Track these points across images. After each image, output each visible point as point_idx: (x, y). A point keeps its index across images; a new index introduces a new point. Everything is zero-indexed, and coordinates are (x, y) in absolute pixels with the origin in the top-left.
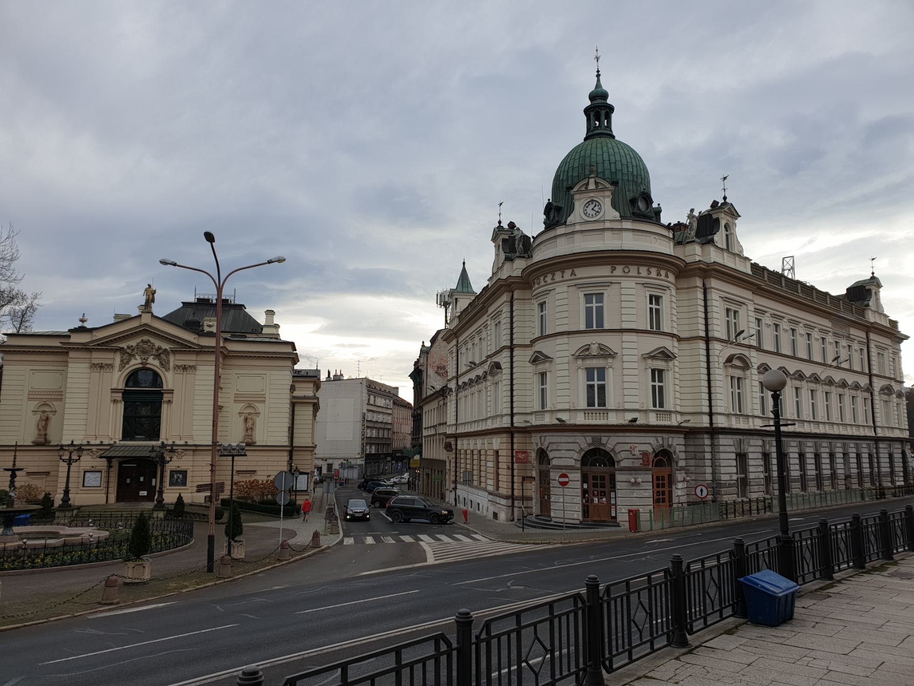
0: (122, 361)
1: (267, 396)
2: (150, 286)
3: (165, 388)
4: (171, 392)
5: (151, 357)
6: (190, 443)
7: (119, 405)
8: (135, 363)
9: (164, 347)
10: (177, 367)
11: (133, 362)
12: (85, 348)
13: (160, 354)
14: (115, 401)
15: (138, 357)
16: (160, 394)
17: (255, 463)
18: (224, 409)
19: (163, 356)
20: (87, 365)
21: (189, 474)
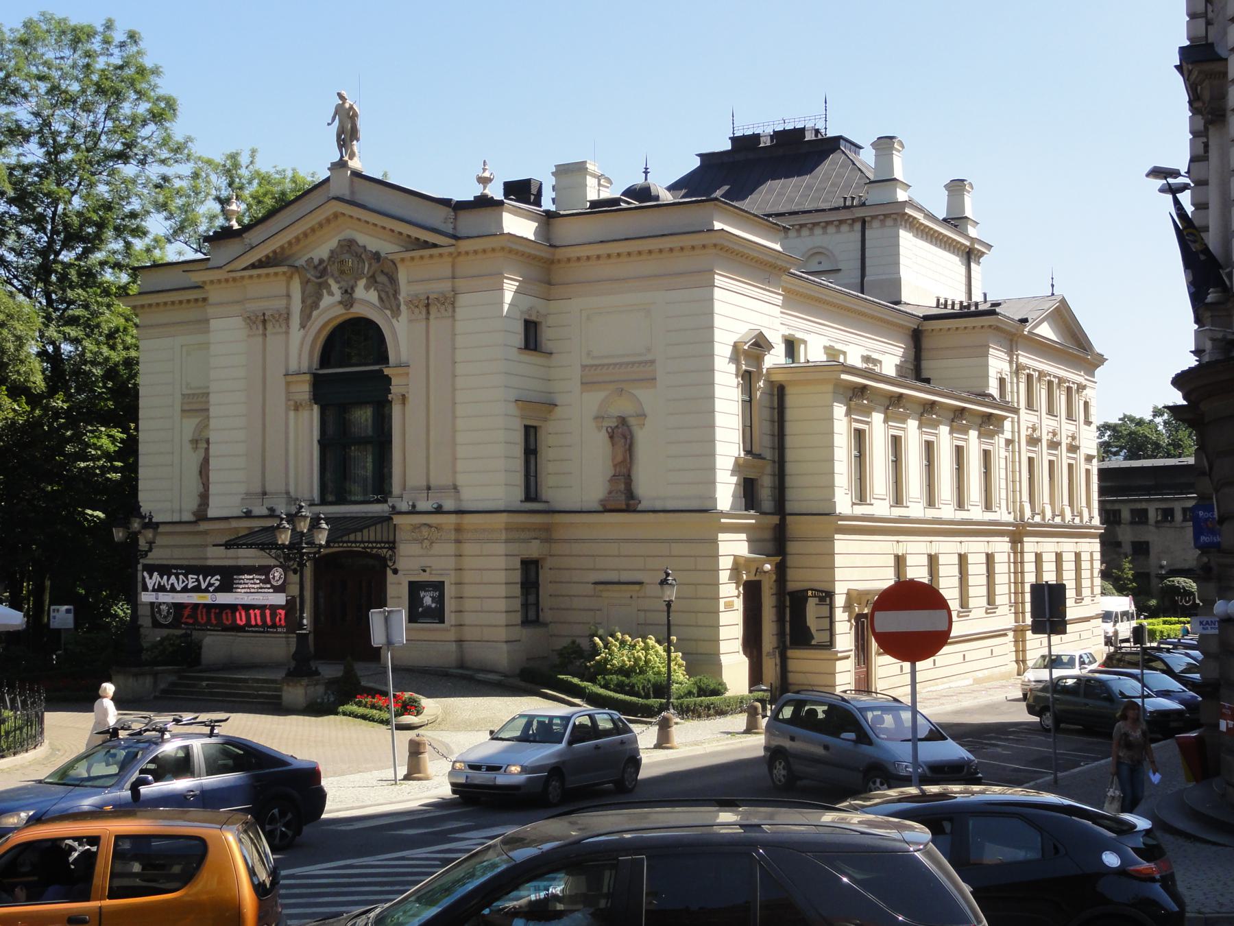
5: (362, 283)
11: (326, 301)
15: (335, 287)
19: (382, 279)
20: (238, 322)
21: (449, 591)
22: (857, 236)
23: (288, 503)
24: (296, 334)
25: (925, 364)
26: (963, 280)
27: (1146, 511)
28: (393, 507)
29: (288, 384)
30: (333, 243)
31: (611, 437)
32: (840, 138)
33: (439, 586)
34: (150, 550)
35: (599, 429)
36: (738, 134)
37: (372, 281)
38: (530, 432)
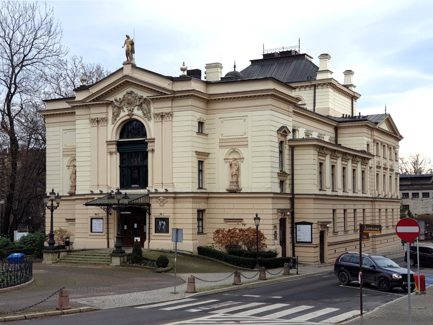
0: (113, 114)
1: (249, 139)
2: (128, 37)
3: (148, 137)
4: (153, 140)
5: (136, 108)
6: (170, 190)
7: (114, 156)
8: (124, 115)
9: (145, 97)
10: (156, 115)
11: (122, 114)
12: (85, 105)
13: (143, 103)
14: (111, 153)
15: (125, 109)
16: (145, 144)
17: (241, 211)
18: (210, 156)
19: (144, 106)
21: (171, 222)
22: (312, 91)
23: (108, 189)
24: (110, 126)
25: (339, 139)
26: (350, 108)
27: (408, 194)
28: (149, 191)
29: (108, 144)
30: (124, 93)
31: (231, 165)
32: (305, 54)
33: (166, 220)
34: (58, 206)
35: (226, 162)
36: (266, 53)
37: (140, 105)
38: (201, 163)
